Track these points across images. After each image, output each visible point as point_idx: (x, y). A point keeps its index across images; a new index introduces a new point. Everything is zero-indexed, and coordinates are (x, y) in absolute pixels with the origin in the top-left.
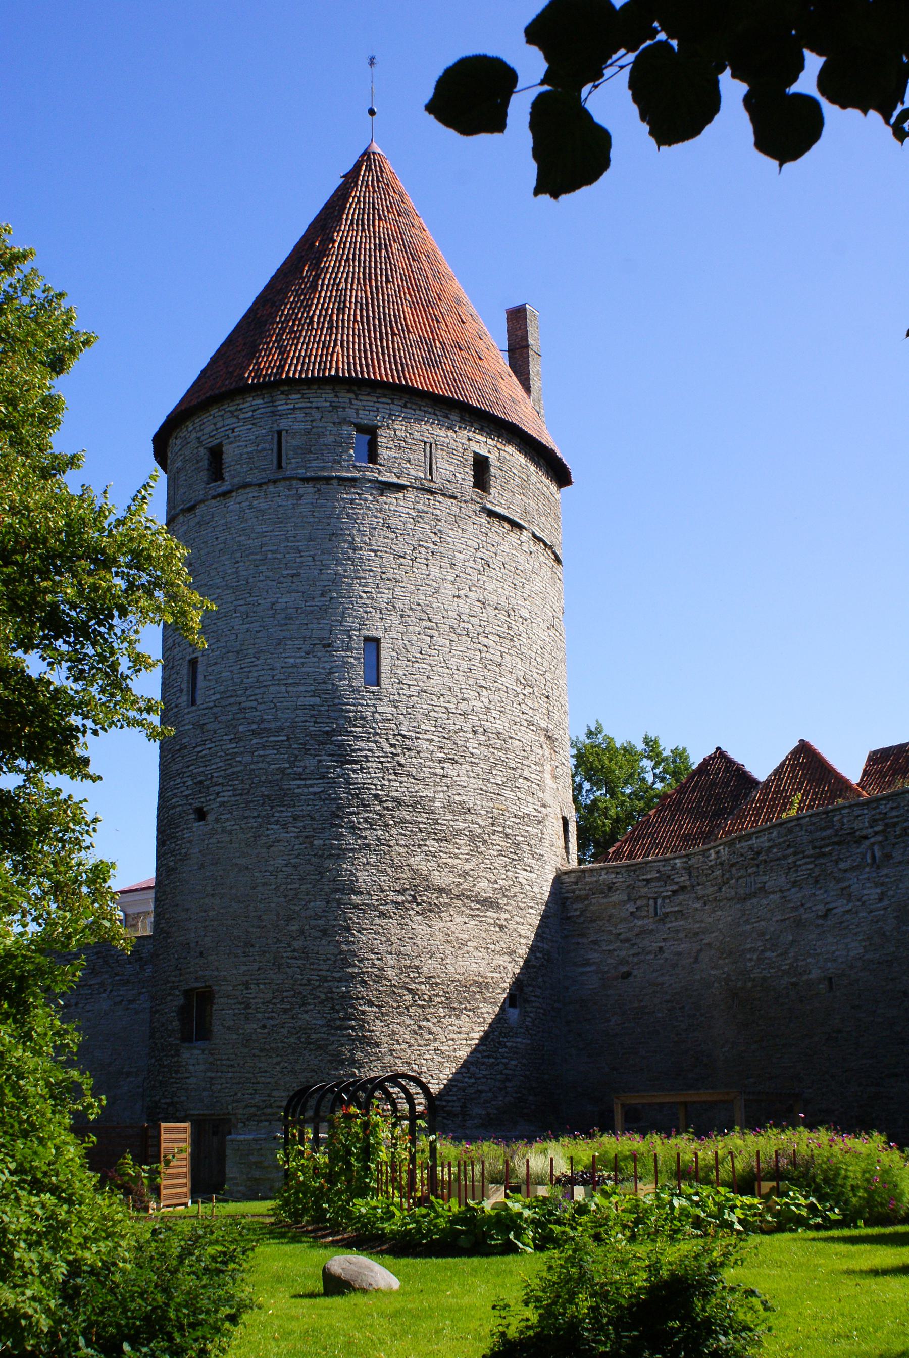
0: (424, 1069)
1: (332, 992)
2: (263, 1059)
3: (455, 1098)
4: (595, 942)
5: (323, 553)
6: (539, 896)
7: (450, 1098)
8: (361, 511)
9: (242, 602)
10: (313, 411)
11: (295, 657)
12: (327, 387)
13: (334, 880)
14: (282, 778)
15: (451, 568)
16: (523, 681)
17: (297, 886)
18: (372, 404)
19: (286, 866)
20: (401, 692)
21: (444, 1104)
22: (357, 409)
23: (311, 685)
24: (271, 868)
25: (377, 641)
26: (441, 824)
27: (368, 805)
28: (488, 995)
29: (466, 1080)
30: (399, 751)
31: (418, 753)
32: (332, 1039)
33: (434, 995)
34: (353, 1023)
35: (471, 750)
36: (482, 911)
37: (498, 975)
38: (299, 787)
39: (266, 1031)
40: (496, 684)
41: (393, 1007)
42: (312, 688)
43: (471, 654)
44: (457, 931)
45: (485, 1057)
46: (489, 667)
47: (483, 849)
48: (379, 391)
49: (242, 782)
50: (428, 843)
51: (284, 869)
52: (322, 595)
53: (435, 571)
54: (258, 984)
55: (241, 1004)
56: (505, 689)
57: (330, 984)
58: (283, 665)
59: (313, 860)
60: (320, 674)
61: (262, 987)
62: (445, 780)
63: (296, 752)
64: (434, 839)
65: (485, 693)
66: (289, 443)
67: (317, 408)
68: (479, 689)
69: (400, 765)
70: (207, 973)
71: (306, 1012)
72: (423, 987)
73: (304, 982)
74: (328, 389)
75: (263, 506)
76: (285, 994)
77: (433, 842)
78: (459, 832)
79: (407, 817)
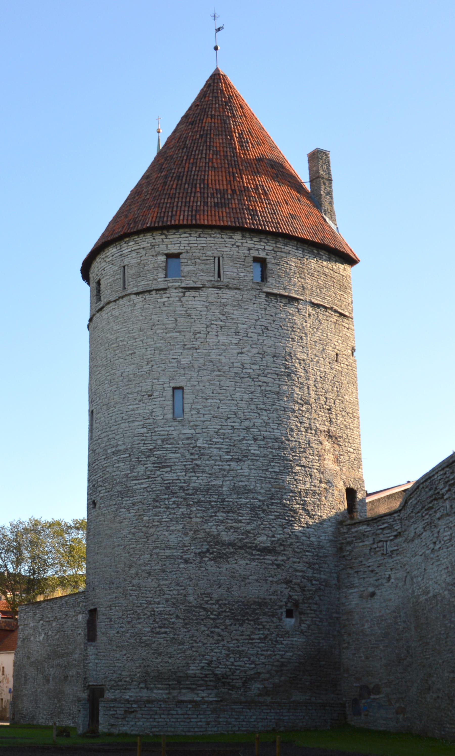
0: (214, 659)
1: (154, 611)
2: (118, 652)
3: (238, 677)
4: (357, 572)
5: (147, 338)
6: (316, 543)
7: (234, 677)
8: (171, 308)
9: (108, 374)
10: (141, 251)
11: (133, 405)
12: (149, 234)
13: (155, 542)
14: (127, 480)
15: (236, 335)
17: (134, 546)
18: (176, 239)
19: (129, 533)
20: (197, 419)
21: (228, 681)
22: (167, 245)
23: (141, 421)
24: (121, 536)
25: (181, 388)
26: (228, 501)
27: (176, 493)
28: (267, 610)
29: (247, 665)
30: (196, 457)
31: (211, 457)
32: (154, 640)
33: (222, 612)
34: (167, 630)
35: (252, 451)
36: (262, 556)
37: (275, 597)
38: (135, 485)
39: (119, 635)
40: (274, 407)
41: (192, 619)
42: (142, 423)
43: (252, 389)
44: (240, 570)
45: (264, 651)
46: (268, 395)
47: (262, 515)
48: (181, 230)
49: (109, 484)
50: (218, 514)
51: (128, 536)
52: (147, 364)
53: (223, 339)
54: (115, 606)
55: (108, 618)
56: (283, 409)
57: (153, 606)
58: (127, 410)
59: (144, 529)
60: (147, 413)
61: (117, 608)
62: (232, 473)
63: (134, 463)
64: (223, 512)
65: (265, 413)
66: (130, 272)
67: (143, 248)
68: (259, 411)
69: (197, 465)
70: (96, 600)
71: (140, 623)
72: (214, 606)
73: (139, 605)
74: (149, 235)
75: (117, 313)
76: (129, 612)
77: (221, 514)
78: (241, 506)
79: (203, 499)
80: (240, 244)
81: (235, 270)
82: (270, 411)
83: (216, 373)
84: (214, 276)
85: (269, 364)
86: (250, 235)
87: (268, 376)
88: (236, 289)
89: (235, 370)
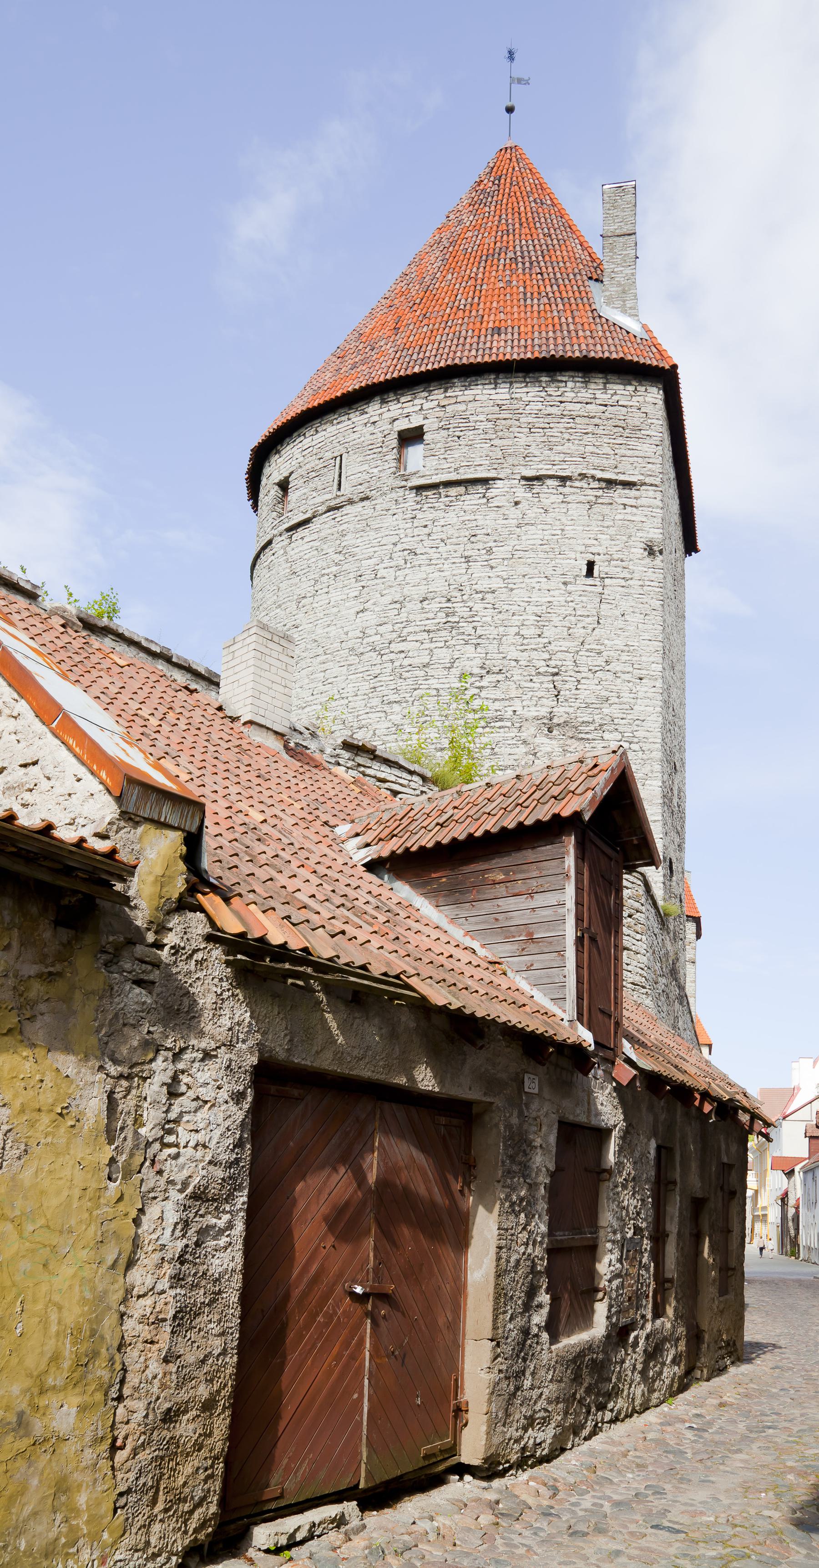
16: (476, 671)
43: (376, 670)
46: (405, 675)
65: (396, 708)
68: (386, 708)
81: (366, 467)
82: (407, 702)
83: (319, 659)
85: (411, 617)
86: (396, 394)
87: (409, 639)
88: (362, 500)
89: (350, 644)
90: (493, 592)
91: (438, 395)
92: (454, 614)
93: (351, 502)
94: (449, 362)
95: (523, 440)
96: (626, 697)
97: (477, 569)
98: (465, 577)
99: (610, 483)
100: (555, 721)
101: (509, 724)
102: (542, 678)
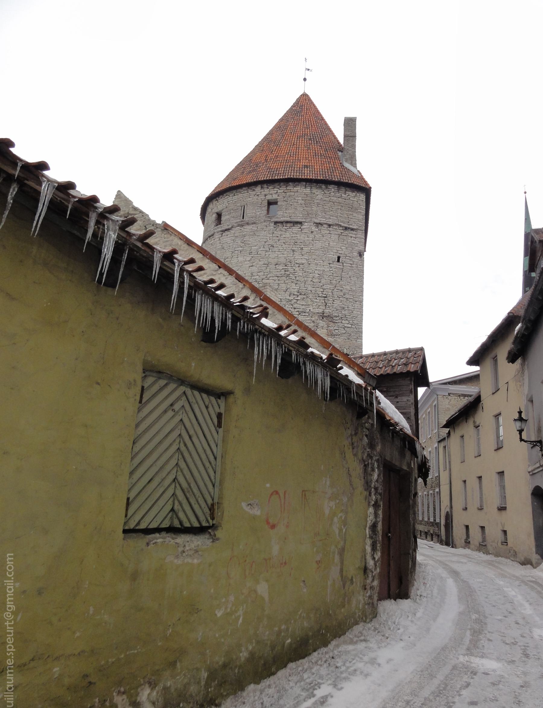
16: (296, 293)
80: (259, 193)
84: (240, 219)
88: (253, 224)
90: (303, 264)
91: (283, 188)
92: (288, 271)
93: (248, 224)
94: (289, 177)
95: (314, 208)
96: (351, 308)
97: (297, 255)
98: (293, 258)
99: (346, 229)
100: (325, 315)
101: (307, 314)
102: (320, 298)
